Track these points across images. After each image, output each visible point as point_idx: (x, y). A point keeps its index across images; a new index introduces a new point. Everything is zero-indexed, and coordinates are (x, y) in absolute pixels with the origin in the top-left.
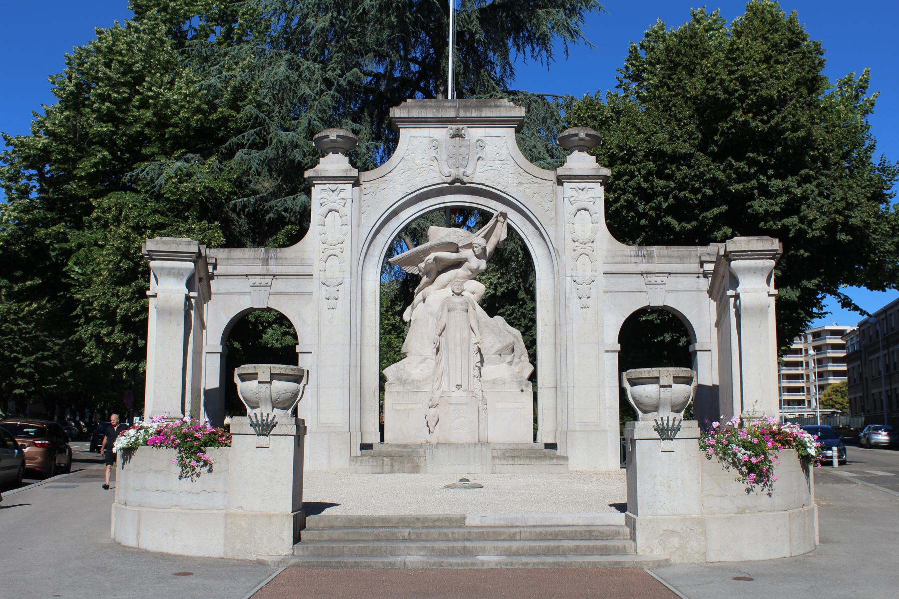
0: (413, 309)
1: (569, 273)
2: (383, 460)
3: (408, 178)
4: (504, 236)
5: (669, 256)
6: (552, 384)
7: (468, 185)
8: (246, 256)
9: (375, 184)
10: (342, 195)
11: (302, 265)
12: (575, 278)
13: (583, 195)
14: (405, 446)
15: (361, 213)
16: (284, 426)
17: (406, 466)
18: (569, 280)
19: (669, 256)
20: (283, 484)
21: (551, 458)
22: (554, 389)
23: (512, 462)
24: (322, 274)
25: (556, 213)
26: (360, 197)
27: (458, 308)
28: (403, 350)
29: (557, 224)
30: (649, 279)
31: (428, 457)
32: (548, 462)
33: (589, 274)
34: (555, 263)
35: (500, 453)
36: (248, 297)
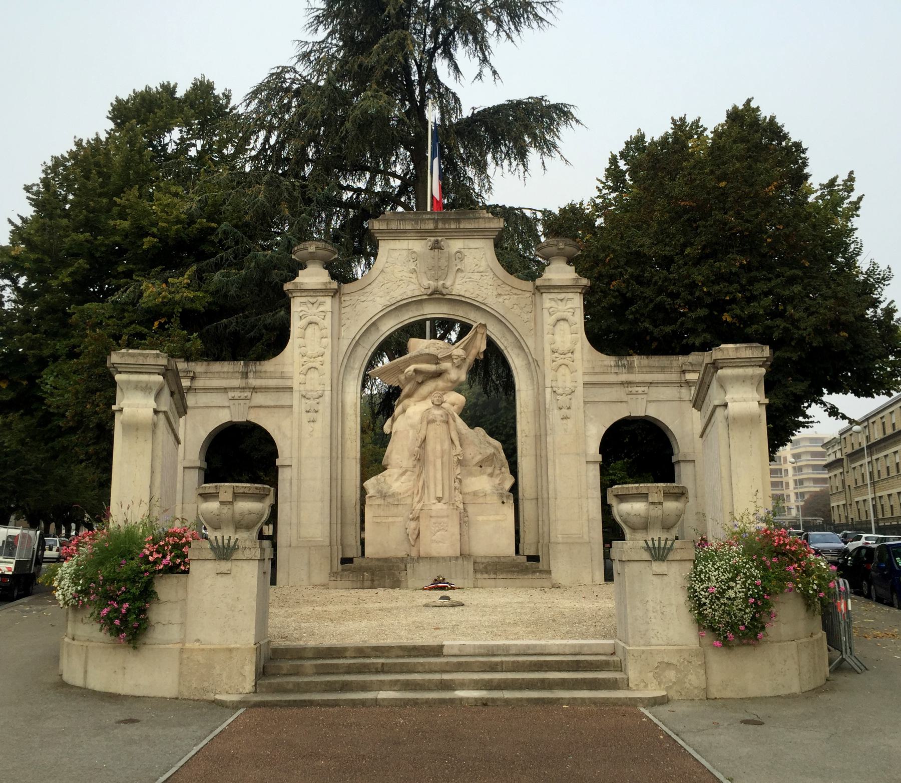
0: (393, 421)
1: (548, 383)
2: (363, 576)
3: (387, 291)
4: (484, 347)
5: (650, 367)
6: (533, 495)
8: (225, 370)
9: (355, 297)
10: (321, 308)
11: (282, 378)
12: (555, 389)
13: (561, 306)
14: (386, 560)
15: (341, 325)
16: (248, 550)
17: (387, 581)
18: (548, 391)
19: (650, 367)
20: (245, 614)
21: (534, 572)
22: (535, 501)
23: (492, 576)
24: (302, 388)
25: (535, 324)
26: (340, 310)
27: (438, 420)
28: (384, 462)
29: (536, 334)
30: (630, 389)
31: (409, 571)
32: (530, 576)
33: (569, 385)
34: (534, 374)
35: (481, 566)
36: (226, 411)
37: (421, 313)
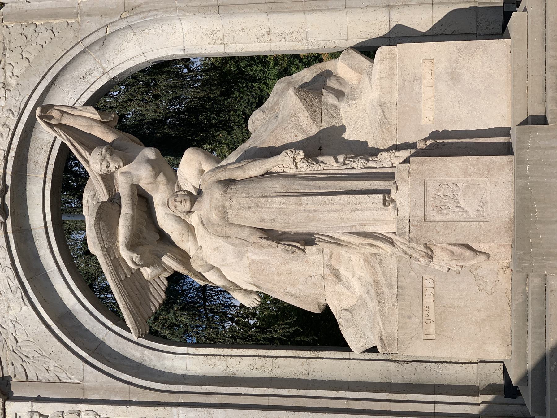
7: (8, 182)
28: (314, 309)
37: (42, 231)
